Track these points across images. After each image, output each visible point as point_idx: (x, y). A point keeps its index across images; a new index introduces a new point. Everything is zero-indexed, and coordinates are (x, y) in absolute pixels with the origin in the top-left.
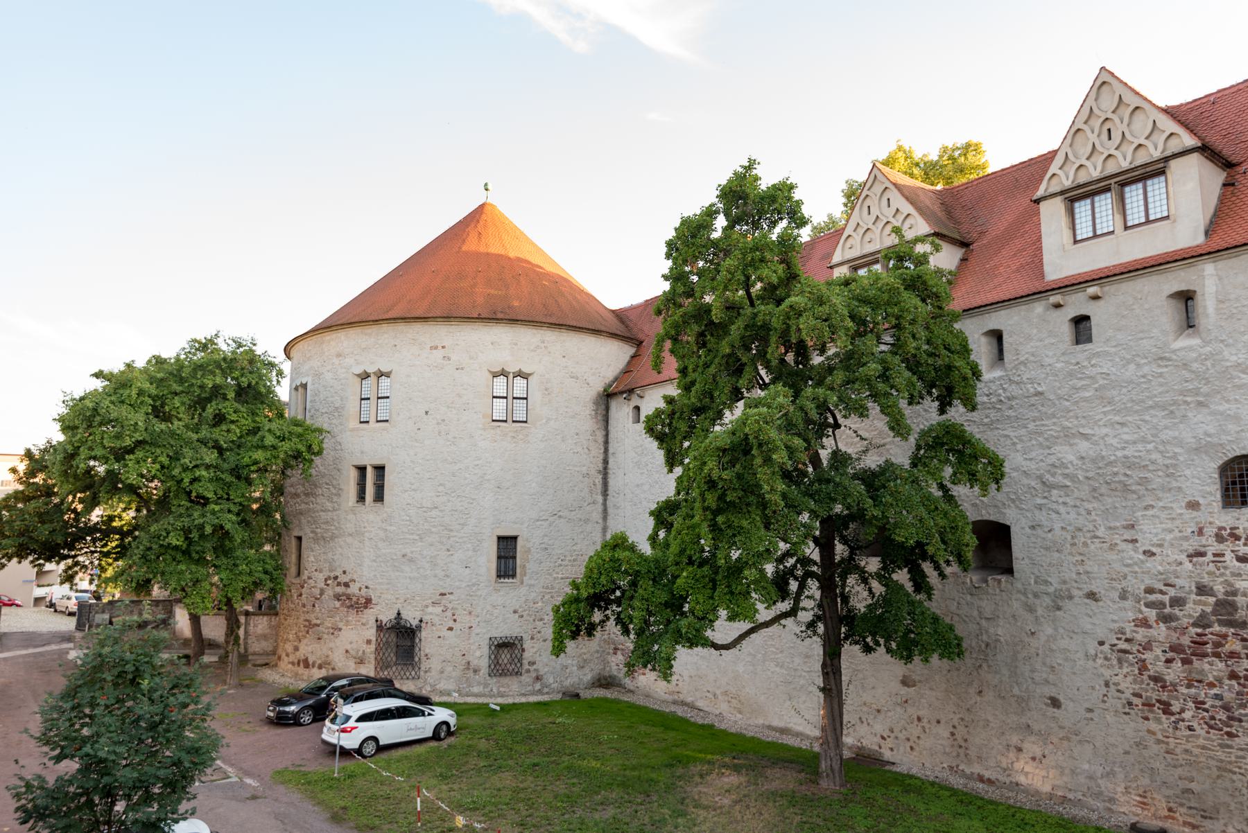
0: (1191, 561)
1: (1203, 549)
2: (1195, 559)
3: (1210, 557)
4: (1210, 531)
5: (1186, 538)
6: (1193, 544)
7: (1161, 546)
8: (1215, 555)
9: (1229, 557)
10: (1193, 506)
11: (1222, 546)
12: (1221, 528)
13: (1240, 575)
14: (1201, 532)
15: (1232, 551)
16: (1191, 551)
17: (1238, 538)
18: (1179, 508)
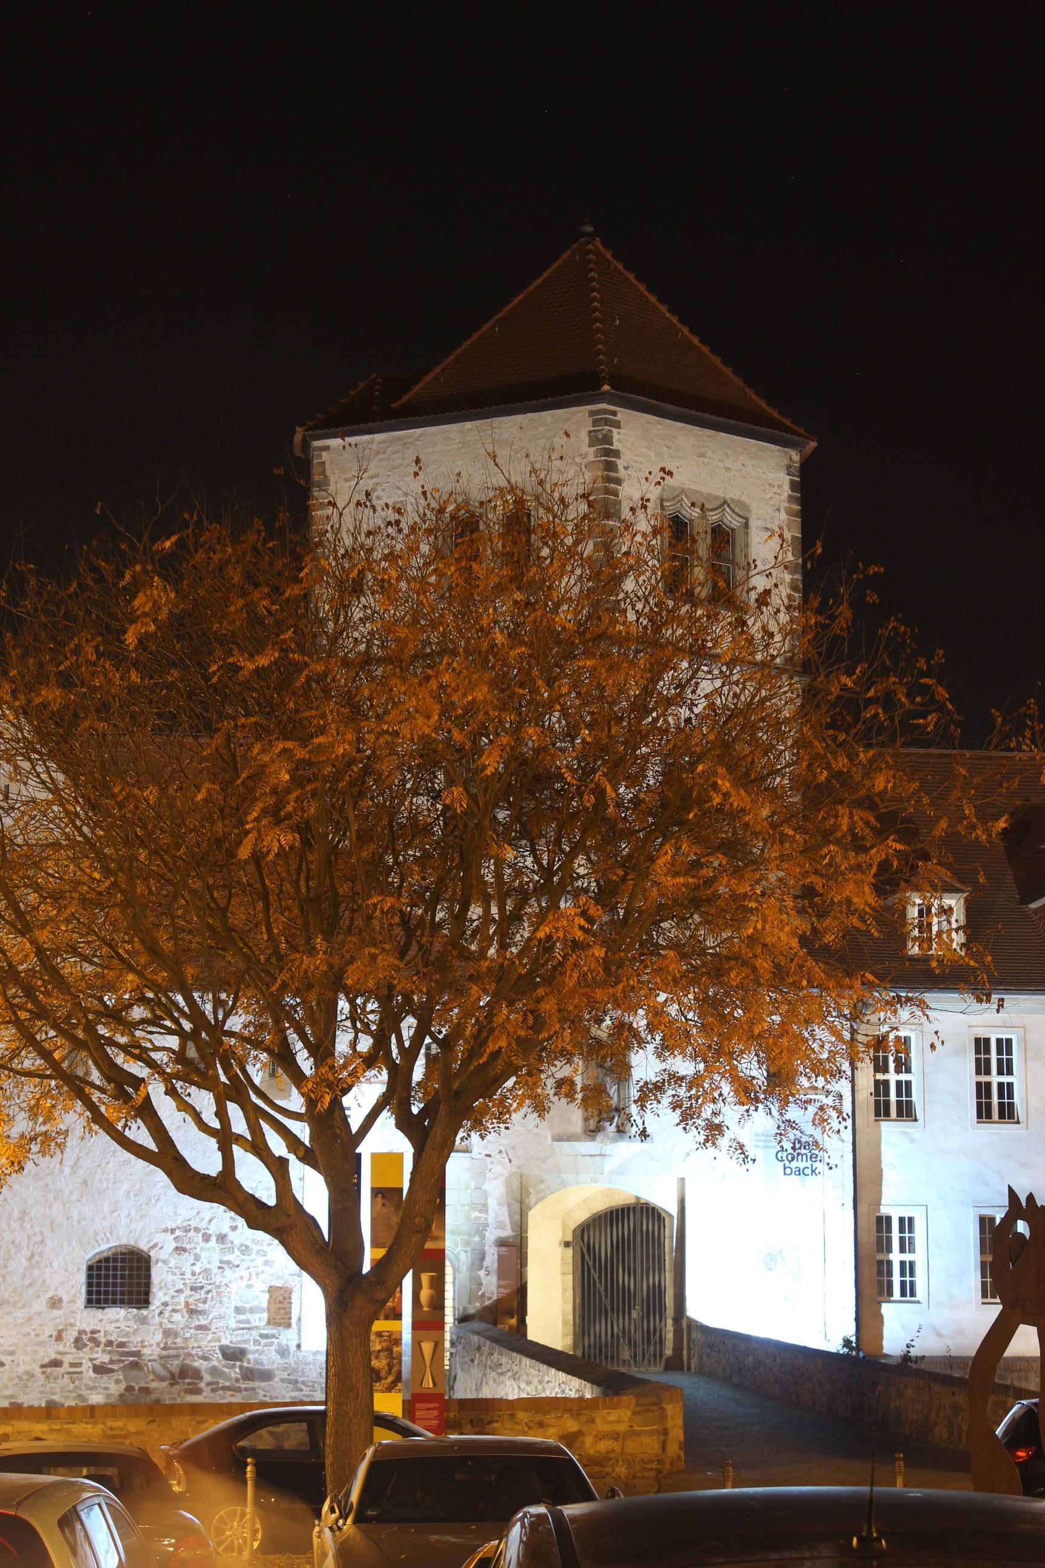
0: (43, 1373)
1: (59, 1357)
2: (49, 1370)
3: (66, 1367)
4: (71, 1336)
5: (41, 1344)
6: (50, 1353)
7: (12, 1353)
8: (72, 1365)
9: (87, 1365)
10: (55, 1303)
11: (81, 1354)
12: (80, 1332)
13: (94, 1388)
14: (59, 1338)
15: (91, 1360)
16: (46, 1360)
17: (97, 1343)
18: (39, 1305)
